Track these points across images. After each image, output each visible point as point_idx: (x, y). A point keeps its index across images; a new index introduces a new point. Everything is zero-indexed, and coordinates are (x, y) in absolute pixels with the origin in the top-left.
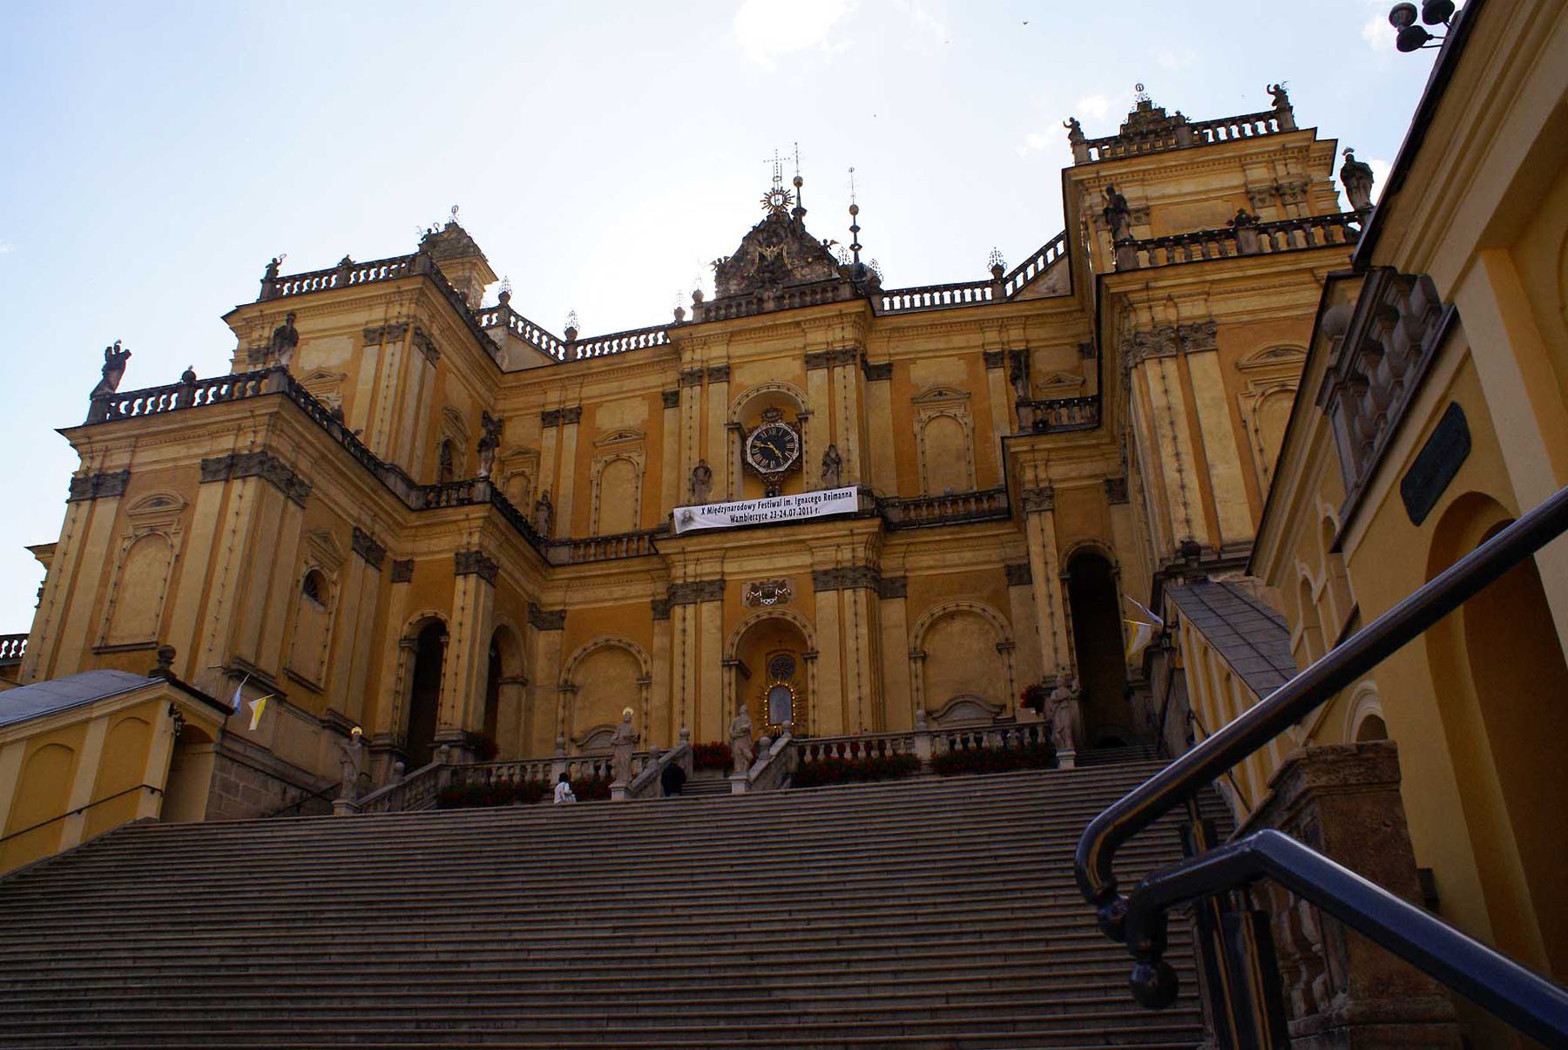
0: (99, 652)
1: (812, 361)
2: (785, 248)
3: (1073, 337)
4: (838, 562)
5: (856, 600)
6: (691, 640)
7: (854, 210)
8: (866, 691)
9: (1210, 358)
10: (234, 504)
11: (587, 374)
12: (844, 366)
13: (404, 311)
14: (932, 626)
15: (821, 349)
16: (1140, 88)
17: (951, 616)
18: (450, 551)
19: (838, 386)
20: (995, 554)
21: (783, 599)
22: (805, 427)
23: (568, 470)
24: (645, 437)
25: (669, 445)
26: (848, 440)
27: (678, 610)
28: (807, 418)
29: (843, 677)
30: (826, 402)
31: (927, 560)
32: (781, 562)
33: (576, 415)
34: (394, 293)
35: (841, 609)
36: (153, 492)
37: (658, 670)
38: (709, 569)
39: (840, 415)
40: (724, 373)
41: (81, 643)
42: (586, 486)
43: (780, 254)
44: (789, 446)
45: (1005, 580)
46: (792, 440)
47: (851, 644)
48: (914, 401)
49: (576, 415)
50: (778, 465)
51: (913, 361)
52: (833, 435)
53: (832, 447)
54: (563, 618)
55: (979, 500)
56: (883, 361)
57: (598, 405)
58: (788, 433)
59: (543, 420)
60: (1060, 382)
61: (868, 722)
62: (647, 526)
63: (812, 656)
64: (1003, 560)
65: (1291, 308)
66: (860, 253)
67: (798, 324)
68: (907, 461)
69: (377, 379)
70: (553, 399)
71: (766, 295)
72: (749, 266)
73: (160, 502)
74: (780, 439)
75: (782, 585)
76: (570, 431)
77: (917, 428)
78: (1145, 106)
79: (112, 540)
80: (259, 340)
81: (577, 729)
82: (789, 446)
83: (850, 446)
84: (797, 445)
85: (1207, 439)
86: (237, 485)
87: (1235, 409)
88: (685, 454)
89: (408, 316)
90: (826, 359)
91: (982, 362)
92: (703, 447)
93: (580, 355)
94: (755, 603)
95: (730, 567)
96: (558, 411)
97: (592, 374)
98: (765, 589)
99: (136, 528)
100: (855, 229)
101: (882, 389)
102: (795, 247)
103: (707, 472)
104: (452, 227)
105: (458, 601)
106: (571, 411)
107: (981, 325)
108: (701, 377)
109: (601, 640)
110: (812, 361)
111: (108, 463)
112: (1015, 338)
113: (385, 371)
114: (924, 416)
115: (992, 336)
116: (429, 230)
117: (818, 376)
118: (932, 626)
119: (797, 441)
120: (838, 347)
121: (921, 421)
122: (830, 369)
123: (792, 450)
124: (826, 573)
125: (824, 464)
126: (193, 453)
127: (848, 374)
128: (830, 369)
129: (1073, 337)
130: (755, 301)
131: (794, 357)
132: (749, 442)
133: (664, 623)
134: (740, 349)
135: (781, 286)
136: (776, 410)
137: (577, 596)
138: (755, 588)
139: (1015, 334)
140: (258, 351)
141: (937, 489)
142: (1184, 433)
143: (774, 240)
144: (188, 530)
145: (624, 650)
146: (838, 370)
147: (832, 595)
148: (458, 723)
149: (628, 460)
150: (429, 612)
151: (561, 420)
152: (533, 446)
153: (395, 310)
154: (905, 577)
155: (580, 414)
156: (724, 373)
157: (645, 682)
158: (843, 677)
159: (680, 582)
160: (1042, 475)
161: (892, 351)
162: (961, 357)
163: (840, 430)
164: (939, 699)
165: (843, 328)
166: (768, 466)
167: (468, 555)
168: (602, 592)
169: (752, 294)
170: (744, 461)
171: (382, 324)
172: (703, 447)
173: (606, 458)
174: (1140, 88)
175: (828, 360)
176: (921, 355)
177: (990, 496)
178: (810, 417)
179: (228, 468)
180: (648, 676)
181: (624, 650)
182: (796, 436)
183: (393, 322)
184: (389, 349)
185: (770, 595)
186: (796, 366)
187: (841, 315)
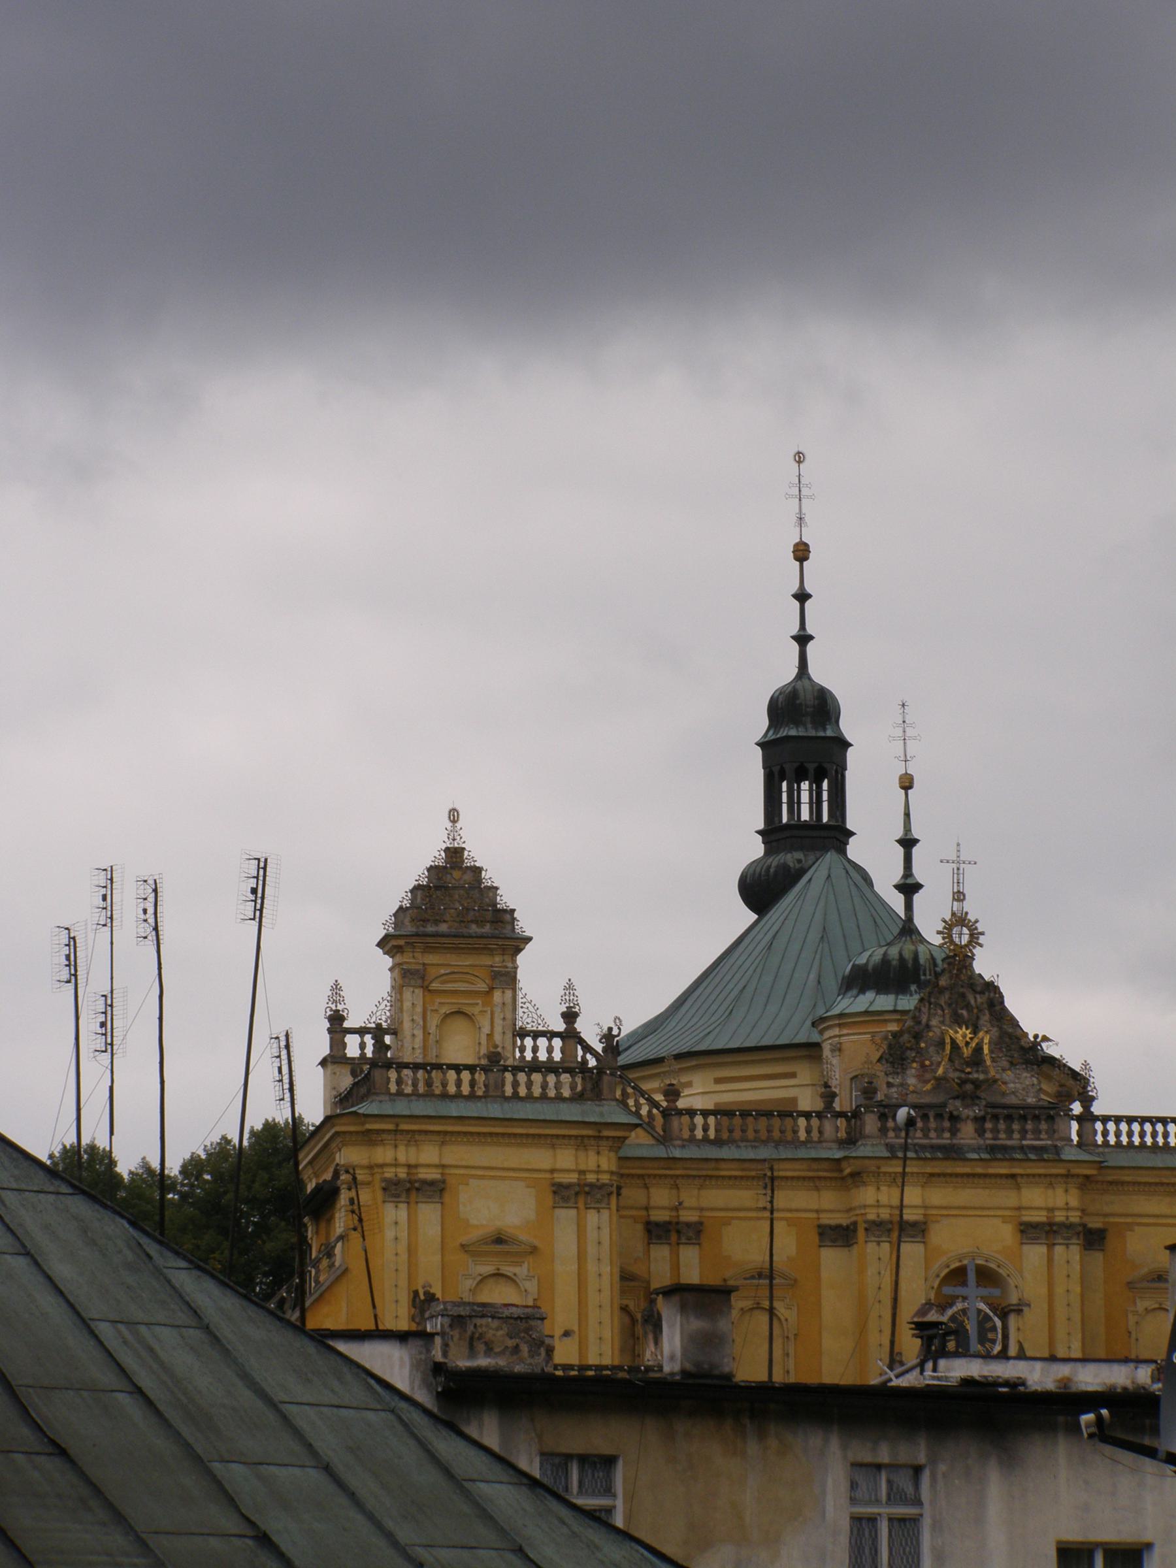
1: (1028, 1231)
2: (986, 1041)
7: (801, 553)
11: (711, 1177)
12: (1067, 1245)
13: (605, 1166)
15: (1039, 1217)
22: (1012, 1320)
26: (1069, 1348)
28: (1021, 1310)
30: (1044, 1291)
34: (589, 1137)
39: (1061, 1312)
40: (917, 1230)
43: (979, 1049)
44: (990, 1336)
46: (994, 1329)
48: (1130, 1285)
51: (1130, 1227)
56: (1095, 1223)
57: (727, 1222)
58: (990, 1319)
59: (649, 1231)
67: (1013, 1176)
69: (581, 1257)
71: (964, 1116)
72: (931, 1049)
77: (1132, 1319)
80: (396, 1165)
82: (990, 1336)
84: (1000, 1336)
89: (612, 1173)
96: (670, 1223)
97: (718, 1177)
100: (802, 597)
102: (995, 1031)
104: (455, 854)
106: (688, 1225)
108: (889, 1231)
110: (1028, 1231)
113: (591, 1249)
114: (1141, 1305)
116: (610, 1029)
117: (1035, 1253)
119: (1000, 1331)
120: (1060, 1217)
121: (1135, 1313)
122: (1051, 1246)
123: (993, 1342)
127: (1069, 1255)
128: (1051, 1246)
130: (946, 1116)
131: (1005, 1220)
134: (938, 1196)
135: (984, 1103)
140: (397, 1183)
143: (964, 1012)
146: (1059, 1250)
151: (674, 1237)
155: (699, 1233)
161: (1107, 1209)
163: (1061, 1333)
165: (1066, 1191)
169: (944, 1105)
175: (1047, 1233)
176: (1139, 1220)
178: (1025, 1309)
182: (999, 1323)
183: (591, 1178)
184: (592, 1218)
186: (1006, 1233)
187: (1068, 1175)
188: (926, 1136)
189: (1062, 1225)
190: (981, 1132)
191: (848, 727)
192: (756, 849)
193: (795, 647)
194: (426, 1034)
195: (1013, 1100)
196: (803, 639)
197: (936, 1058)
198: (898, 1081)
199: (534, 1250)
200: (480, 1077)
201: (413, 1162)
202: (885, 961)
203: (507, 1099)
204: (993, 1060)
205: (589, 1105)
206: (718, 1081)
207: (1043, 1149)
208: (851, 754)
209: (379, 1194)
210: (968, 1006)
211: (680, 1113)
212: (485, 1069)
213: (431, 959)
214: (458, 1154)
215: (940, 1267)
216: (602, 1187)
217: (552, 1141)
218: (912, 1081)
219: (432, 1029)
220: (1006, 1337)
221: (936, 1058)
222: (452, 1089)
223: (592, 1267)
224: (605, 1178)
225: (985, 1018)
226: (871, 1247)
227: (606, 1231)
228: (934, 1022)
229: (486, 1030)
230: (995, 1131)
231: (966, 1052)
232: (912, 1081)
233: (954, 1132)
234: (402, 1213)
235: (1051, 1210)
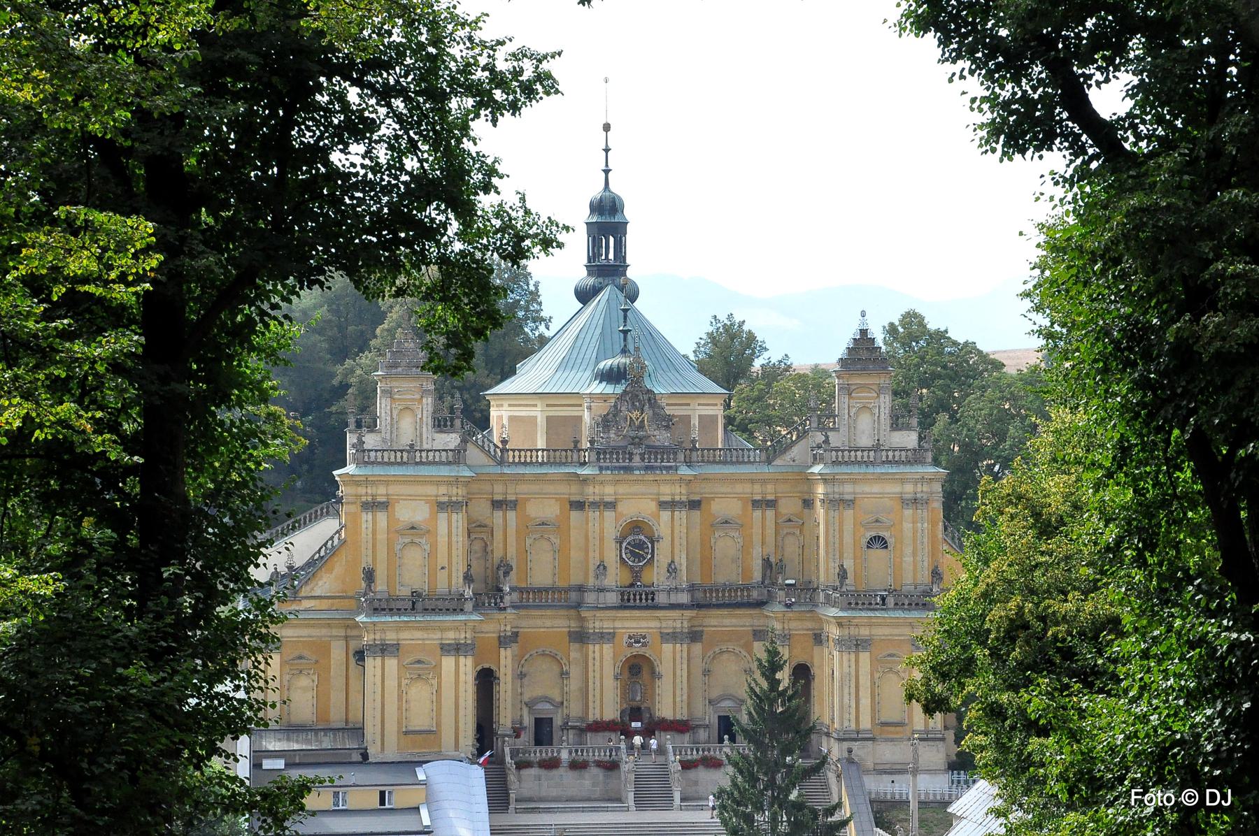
0: (406, 733)
1: (663, 505)
3: (800, 492)
4: (675, 628)
5: (681, 649)
6: (597, 664)
7: (607, 128)
8: (685, 697)
9: (868, 654)
10: (462, 669)
14: (714, 658)
15: (668, 498)
16: (863, 314)
17: (722, 652)
18: (494, 632)
19: (677, 523)
20: (748, 621)
21: (644, 645)
23: (512, 540)
24: (560, 527)
25: (575, 536)
27: (591, 647)
29: (674, 688)
31: (714, 622)
32: (644, 624)
33: (513, 505)
35: (674, 653)
36: (418, 657)
37: (575, 672)
38: (607, 626)
40: (612, 505)
41: (395, 728)
42: (524, 552)
43: (643, 421)
45: (751, 638)
47: (678, 672)
48: (712, 525)
49: (513, 505)
50: (640, 561)
51: (713, 499)
52: (672, 552)
53: (673, 562)
54: (517, 636)
55: (742, 590)
56: (697, 498)
57: (528, 499)
60: (790, 520)
61: (685, 711)
62: (560, 584)
63: (660, 677)
64: (752, 626)
65: (900, 635)
66: (610, 174)
68: (707, 561)
70: (499, 492)
71: (635, 451)
73: (419, 662)
74: (641, 545)
75: (644, 637)
76: (511, 515)
77: (713, 541)
78: (864, 332)
79: (400, 679)
81: (526, 698)
83: (682, 561)
85: (861, 688)
86: (462, 659)
87: (872, 675)
88: (591, 554)
90: (671, 505)
91: (750, 503)
92: (601, 553)
93: (511, 460)
94: (630, 645)
95: (618, 624)
98: (636, 639)
99: (410, 674)
100: (607, 150)
101: (696, 514)
102: (651, 412)
103: (605, 568)
105: (502, 662)
106: (511, 501)
107: (753, 481)
109: (540, 650)
110: (663, 505)
111: (383, 637)
112: (770, 492)
113: (454, 530)
115: (757, 488)
117: (665, 515)
118: (714, 658)
120: (677, 498)
122: (673, 512)
124: (668, 634)
125: (668, 571)
126: (434, 638)
127: (681, 515)
128: (673, 512)
129: (800, 492)
131: (652, 500)
132: (624, 545)
133: (577, 645)
134: (622, 489)
136: (639, 527)
137: (524, 623)
138: (630, 637)
139: (770, 488)
141: (721, 578)
142: (853, 685)
144: (440, 677)
145: (554, 657)
147: (670, 646)
148: (509, 725)
149: (549, 540)
150: (486, 666)
152: (488, 522)
153: (455, 491)
154: (702, 631)
156: (612, 505)
157: (564, 675)
158: (674, 688)
159: (591, 631)
160: (786, 627)
162: (739, 499)
163: (676, 551)
164: (715, 694)
166: (634, 562)
167: (505, 637)
168: (539, 622)
170: (621, 555)
171: (446, 499)
172: (601, 553)
173: (534, 536)
174: (863, 314)
177: (747, 588)
179: (456, 649)
180: (567, 673)
181: (554, 657)
183: (454, 499)
184: (454, 516)
185: (639, 642)
188: (618, 461)
189: (678, 502)
190: (643, 459)
191: (629, 213)
192: (584, 272)
193: (603, 175)
194: (392, 418)
195: (657, 444)
196: (607, 172)
197: (624, 425)
198: (605, 436)
199: (428, 531)
200: (405, 455)
201: (374, 493)
202: (611, 368)
203: (417, 463)
204: (649, 426)
205: (454, 467)
206: (547, 405)
207: (671, 467)
208: (628, 226)
209: (360, 508)
210: (639, 400)
211: (508, 451)
212: (408, 452)
213: (394, 384)
214: (393, 489)
215: (622, 522)
216: (457, 503)
217: (438, 483)
218: (612, 436)
219: (395, 417)
220: (653, 551)
221: (624, 425)
222: (393, 459)
223: (454, 539)
224: (460, 499)
225: (647, 406)
226: (591, 514)
227: (460, 524)
228: (623, 409)
229: (419, 416)
230: (650, 458)
231: (637, 423)
232: (612, 436)
233: (630, 460)
234: (370, 516)
235: (673, 495)
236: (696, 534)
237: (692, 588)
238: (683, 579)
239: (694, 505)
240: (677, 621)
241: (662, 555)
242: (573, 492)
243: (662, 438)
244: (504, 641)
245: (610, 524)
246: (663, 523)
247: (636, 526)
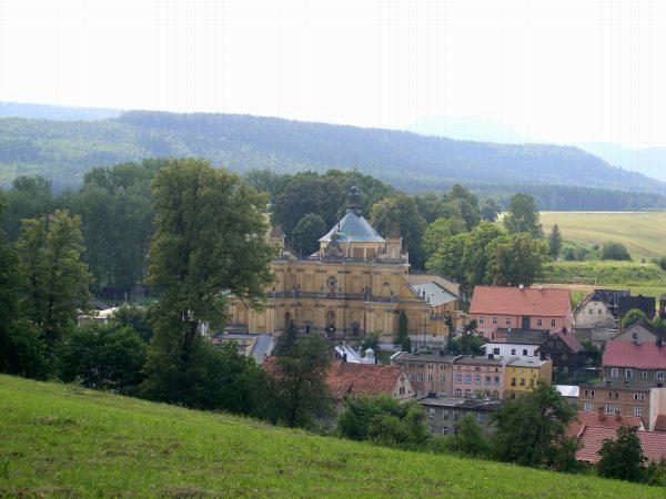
5: (342, 310)
42: (305, 283)
90: (340, 272)
98: (331, 307)
236: (348, 281)
237: (346, 294)
238: (343, 292)
239: (348, 272)
240: (341, 303)
241: (338, 285)
242: (316, 268)
243: (339, 255)
244: (292, 305)
245: (324, 277)
246: (338, 277)
247: (332, 277)
